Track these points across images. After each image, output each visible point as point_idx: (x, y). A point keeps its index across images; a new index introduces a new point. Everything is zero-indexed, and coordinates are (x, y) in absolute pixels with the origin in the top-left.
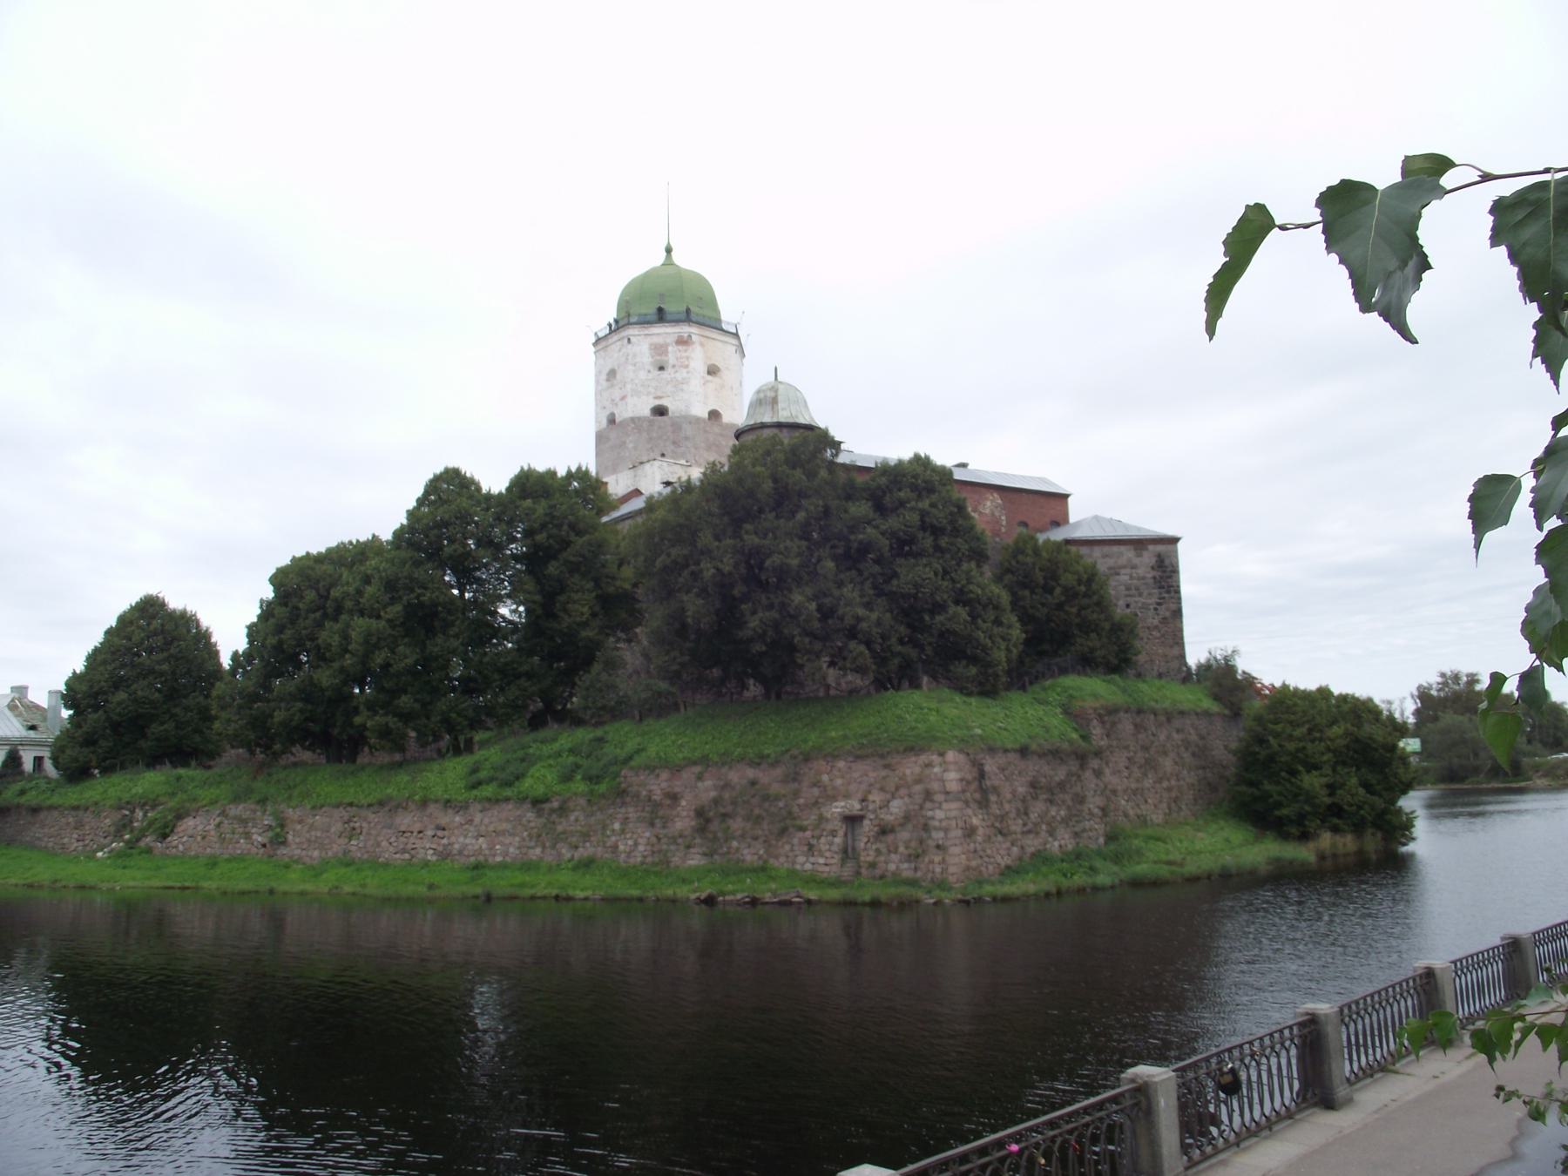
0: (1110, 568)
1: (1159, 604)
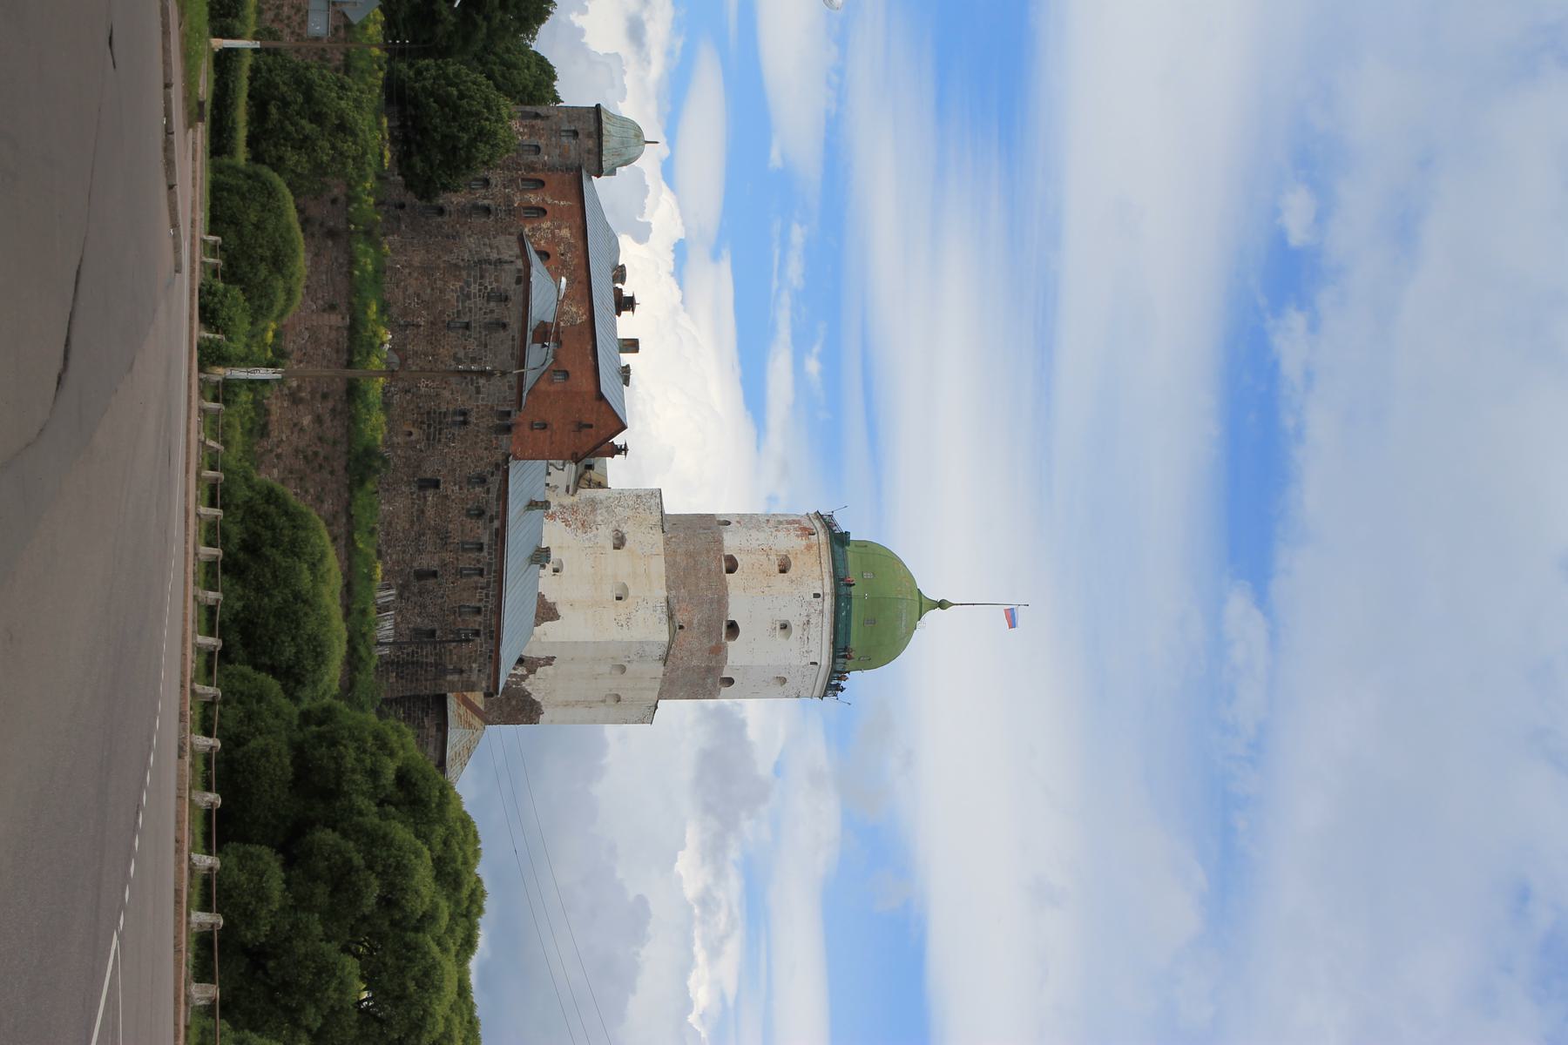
0: (497, 247)
1: (463, 260)
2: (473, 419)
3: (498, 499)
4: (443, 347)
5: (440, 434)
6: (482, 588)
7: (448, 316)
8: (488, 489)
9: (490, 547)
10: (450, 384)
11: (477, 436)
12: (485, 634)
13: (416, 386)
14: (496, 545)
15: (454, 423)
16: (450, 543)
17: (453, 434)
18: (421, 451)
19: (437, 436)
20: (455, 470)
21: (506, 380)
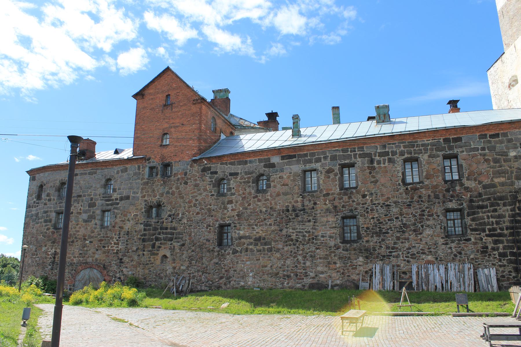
2: (154, 200)
3: (246, 163)
4: (78, 231)
5: (166, 229)
6: (372, 161)
7: (48, 229)
8: (231, 174)
9: (310, 162)
10: (116, 223)
11: (173, 193)
12: (451, 148)
13: (117, 253)
14: (306, 155)
15: (158, 215)
16: (303, 206)
17: (170, 216)
18: (183, 245)
19: (169, 231)
20: (209, 210)
21: (116, 176)
